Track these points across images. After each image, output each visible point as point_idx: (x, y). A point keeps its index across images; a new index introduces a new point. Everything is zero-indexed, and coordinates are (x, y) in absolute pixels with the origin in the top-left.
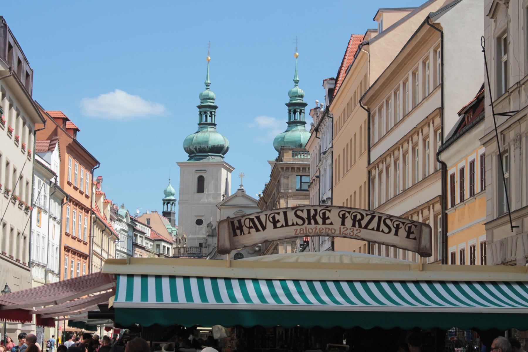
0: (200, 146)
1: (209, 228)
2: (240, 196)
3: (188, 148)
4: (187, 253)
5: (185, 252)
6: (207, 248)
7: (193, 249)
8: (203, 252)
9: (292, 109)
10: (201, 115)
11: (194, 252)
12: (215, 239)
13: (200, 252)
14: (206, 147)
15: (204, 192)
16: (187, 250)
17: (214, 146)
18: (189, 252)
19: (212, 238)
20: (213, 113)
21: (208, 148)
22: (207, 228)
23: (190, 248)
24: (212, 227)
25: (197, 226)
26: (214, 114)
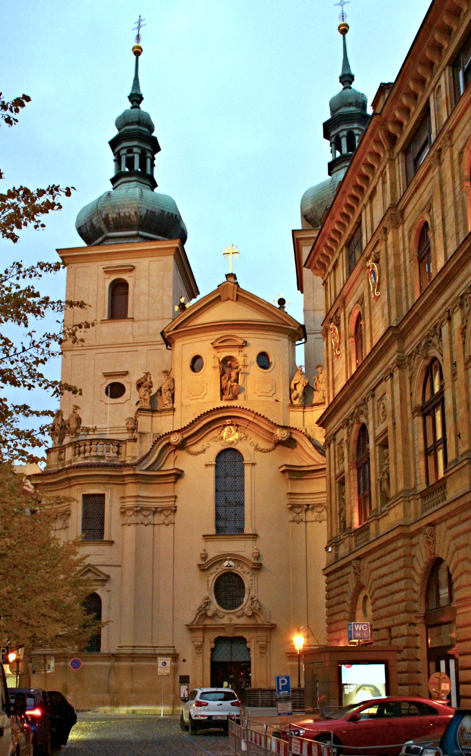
0: (117, 211)
1: (142, 390)
3: (89, 224)
4: (82, 455)
5: (75, 455)
6: (138, 441)
7: (99, 446)
8: (126, 454)
10: (118, 161)
11: (100, 454)
12: (159, 418)
13: (118, 453)
14: (133, 214)
17: (153, 213)
18: (87, 454)
19: (152, 416)
20: (149, 155)
21: (137, 217)
22: (138, 390)
23: (91, 444)
24: (150, 387)
25: (109, 400)
26: (150, 158)
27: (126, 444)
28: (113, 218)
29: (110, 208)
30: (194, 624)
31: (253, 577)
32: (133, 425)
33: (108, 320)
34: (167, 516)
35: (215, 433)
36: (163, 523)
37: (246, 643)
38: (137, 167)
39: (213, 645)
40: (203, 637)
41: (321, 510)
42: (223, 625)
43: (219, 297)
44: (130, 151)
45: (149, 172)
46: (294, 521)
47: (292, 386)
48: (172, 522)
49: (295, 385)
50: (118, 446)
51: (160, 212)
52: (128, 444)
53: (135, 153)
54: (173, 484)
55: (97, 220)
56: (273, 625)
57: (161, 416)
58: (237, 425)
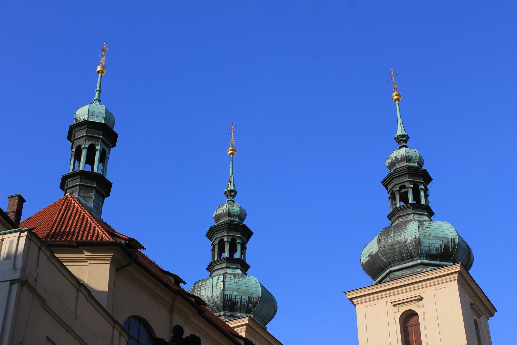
10: (393, 197)
20: (422, 187)
38: (411, 200)
45: (423, 202)
53: (407, 188)
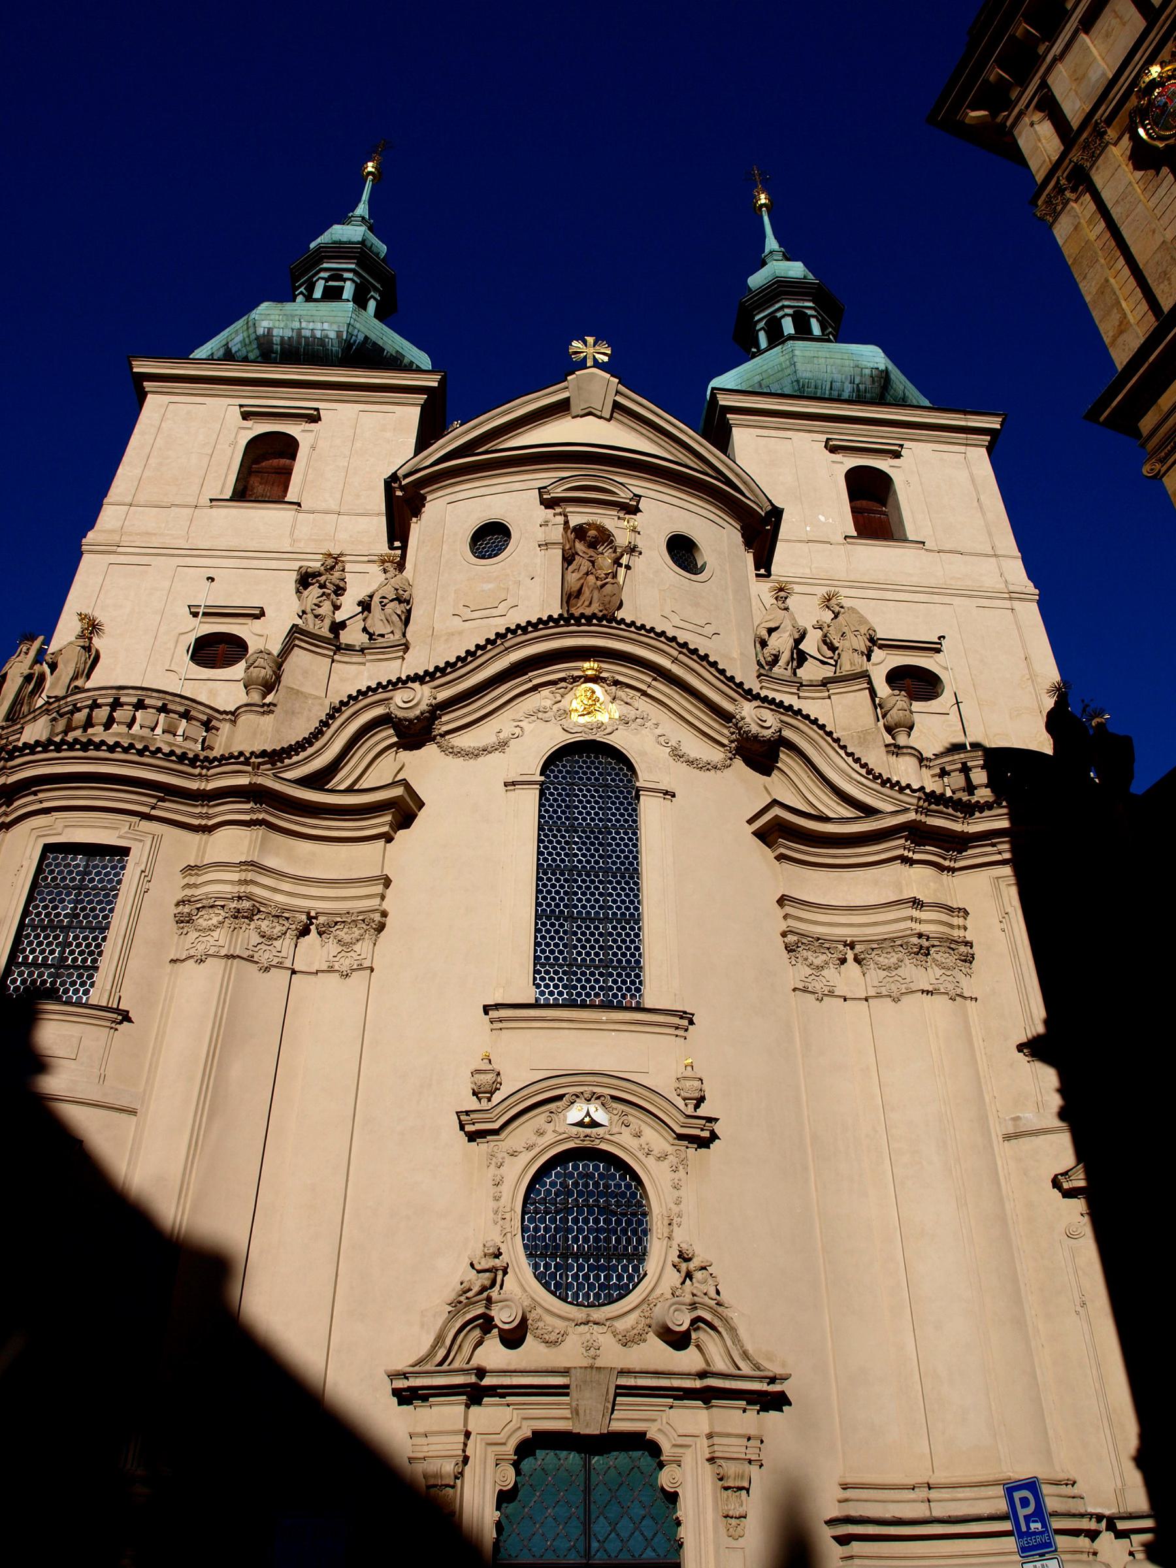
0: (296, 325)
1: (314, 592)
2: (590, 414)
3: (222, 352)
9: (783, 307)
14: (332, 335)
15: (286, 499)
16: (81, 717)
22: (298, 591)
24: (340, 590)
27: (234, 722)
28: (282, 338)
29: (277, 317)
30: (429, 1367)
31: (682, 1173)
32: (270, 672)
33: (231, 500)
34: (346, 945)
35: (544, 698)
36: (331, 970)
37: (661, 1465)
39: (509, 1477)
40: (468, 1435)
41: (894, 960)
42: (566, 1372)
43: (567, 400)
44: (337, 276)
46: (805, 990)
47: (764, 633)
48: (367, 964)
49: (771, 631)
50: (207, 725)
51: (394, 354)
52: (242, 719)
53: (345, 280)
54: (382, 842)
55: (243, 342)
56: (772, 1380)
57: (364, 664)
58: (616, 683)
